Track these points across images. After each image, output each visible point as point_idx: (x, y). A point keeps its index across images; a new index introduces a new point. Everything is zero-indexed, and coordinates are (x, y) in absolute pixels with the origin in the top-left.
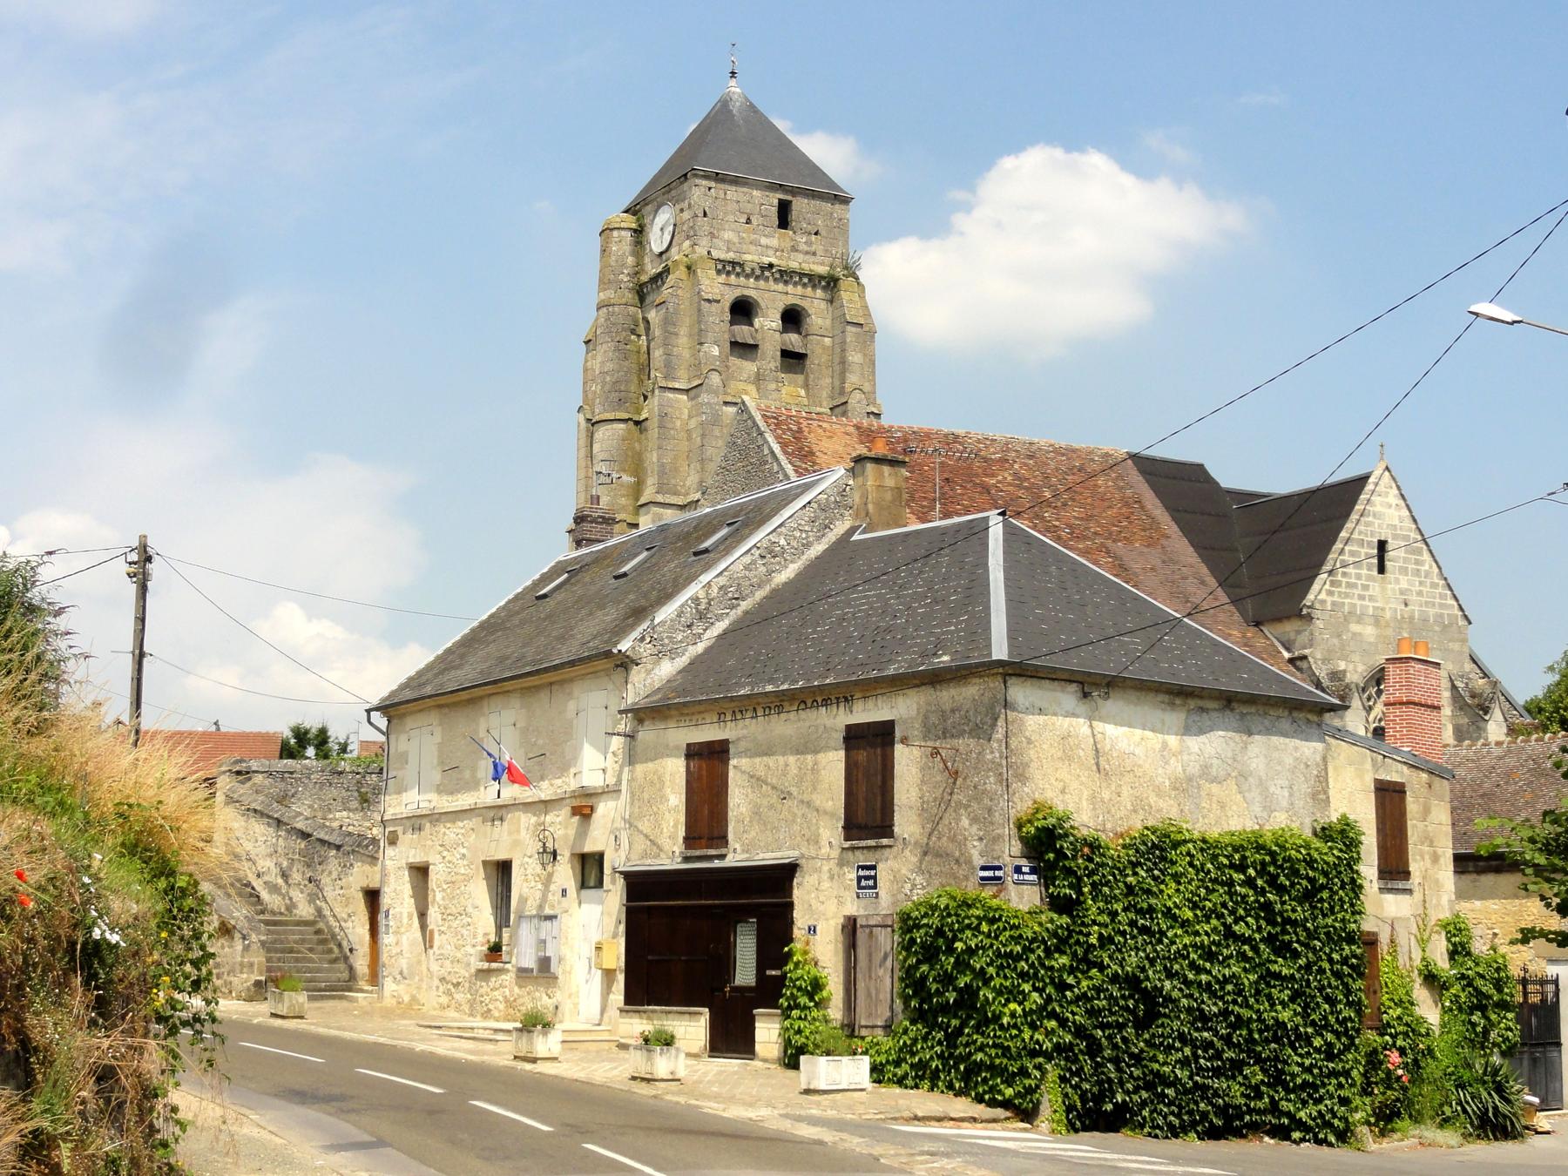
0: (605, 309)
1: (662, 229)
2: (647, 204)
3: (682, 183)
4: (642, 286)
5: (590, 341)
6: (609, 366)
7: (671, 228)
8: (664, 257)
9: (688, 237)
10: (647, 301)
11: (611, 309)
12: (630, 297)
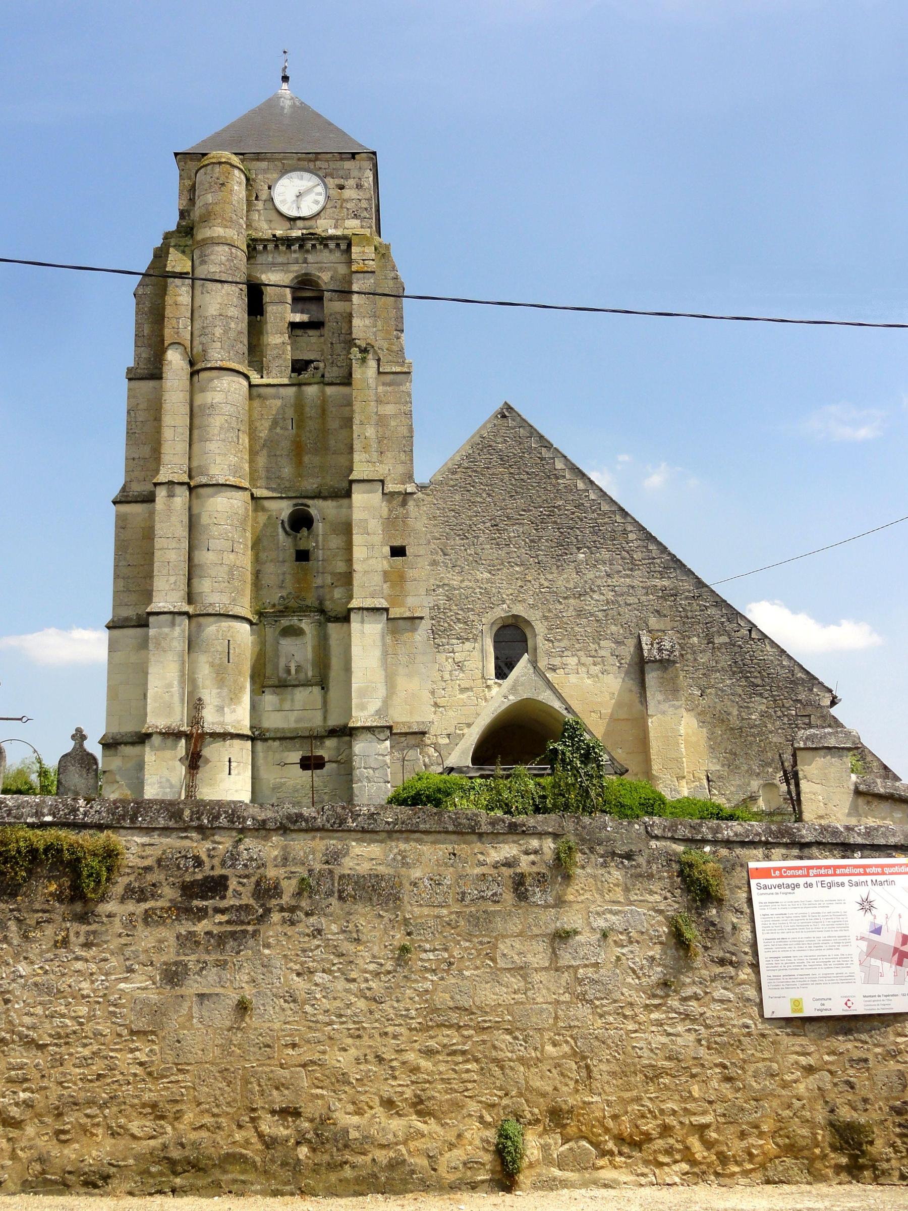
0: (226, 248)
2: (258, 160)
3: (342, 159)
4: (254, 240)
8: (300, 223)
9: (356, 216)
10: (261, 259)
11: (234, 250)
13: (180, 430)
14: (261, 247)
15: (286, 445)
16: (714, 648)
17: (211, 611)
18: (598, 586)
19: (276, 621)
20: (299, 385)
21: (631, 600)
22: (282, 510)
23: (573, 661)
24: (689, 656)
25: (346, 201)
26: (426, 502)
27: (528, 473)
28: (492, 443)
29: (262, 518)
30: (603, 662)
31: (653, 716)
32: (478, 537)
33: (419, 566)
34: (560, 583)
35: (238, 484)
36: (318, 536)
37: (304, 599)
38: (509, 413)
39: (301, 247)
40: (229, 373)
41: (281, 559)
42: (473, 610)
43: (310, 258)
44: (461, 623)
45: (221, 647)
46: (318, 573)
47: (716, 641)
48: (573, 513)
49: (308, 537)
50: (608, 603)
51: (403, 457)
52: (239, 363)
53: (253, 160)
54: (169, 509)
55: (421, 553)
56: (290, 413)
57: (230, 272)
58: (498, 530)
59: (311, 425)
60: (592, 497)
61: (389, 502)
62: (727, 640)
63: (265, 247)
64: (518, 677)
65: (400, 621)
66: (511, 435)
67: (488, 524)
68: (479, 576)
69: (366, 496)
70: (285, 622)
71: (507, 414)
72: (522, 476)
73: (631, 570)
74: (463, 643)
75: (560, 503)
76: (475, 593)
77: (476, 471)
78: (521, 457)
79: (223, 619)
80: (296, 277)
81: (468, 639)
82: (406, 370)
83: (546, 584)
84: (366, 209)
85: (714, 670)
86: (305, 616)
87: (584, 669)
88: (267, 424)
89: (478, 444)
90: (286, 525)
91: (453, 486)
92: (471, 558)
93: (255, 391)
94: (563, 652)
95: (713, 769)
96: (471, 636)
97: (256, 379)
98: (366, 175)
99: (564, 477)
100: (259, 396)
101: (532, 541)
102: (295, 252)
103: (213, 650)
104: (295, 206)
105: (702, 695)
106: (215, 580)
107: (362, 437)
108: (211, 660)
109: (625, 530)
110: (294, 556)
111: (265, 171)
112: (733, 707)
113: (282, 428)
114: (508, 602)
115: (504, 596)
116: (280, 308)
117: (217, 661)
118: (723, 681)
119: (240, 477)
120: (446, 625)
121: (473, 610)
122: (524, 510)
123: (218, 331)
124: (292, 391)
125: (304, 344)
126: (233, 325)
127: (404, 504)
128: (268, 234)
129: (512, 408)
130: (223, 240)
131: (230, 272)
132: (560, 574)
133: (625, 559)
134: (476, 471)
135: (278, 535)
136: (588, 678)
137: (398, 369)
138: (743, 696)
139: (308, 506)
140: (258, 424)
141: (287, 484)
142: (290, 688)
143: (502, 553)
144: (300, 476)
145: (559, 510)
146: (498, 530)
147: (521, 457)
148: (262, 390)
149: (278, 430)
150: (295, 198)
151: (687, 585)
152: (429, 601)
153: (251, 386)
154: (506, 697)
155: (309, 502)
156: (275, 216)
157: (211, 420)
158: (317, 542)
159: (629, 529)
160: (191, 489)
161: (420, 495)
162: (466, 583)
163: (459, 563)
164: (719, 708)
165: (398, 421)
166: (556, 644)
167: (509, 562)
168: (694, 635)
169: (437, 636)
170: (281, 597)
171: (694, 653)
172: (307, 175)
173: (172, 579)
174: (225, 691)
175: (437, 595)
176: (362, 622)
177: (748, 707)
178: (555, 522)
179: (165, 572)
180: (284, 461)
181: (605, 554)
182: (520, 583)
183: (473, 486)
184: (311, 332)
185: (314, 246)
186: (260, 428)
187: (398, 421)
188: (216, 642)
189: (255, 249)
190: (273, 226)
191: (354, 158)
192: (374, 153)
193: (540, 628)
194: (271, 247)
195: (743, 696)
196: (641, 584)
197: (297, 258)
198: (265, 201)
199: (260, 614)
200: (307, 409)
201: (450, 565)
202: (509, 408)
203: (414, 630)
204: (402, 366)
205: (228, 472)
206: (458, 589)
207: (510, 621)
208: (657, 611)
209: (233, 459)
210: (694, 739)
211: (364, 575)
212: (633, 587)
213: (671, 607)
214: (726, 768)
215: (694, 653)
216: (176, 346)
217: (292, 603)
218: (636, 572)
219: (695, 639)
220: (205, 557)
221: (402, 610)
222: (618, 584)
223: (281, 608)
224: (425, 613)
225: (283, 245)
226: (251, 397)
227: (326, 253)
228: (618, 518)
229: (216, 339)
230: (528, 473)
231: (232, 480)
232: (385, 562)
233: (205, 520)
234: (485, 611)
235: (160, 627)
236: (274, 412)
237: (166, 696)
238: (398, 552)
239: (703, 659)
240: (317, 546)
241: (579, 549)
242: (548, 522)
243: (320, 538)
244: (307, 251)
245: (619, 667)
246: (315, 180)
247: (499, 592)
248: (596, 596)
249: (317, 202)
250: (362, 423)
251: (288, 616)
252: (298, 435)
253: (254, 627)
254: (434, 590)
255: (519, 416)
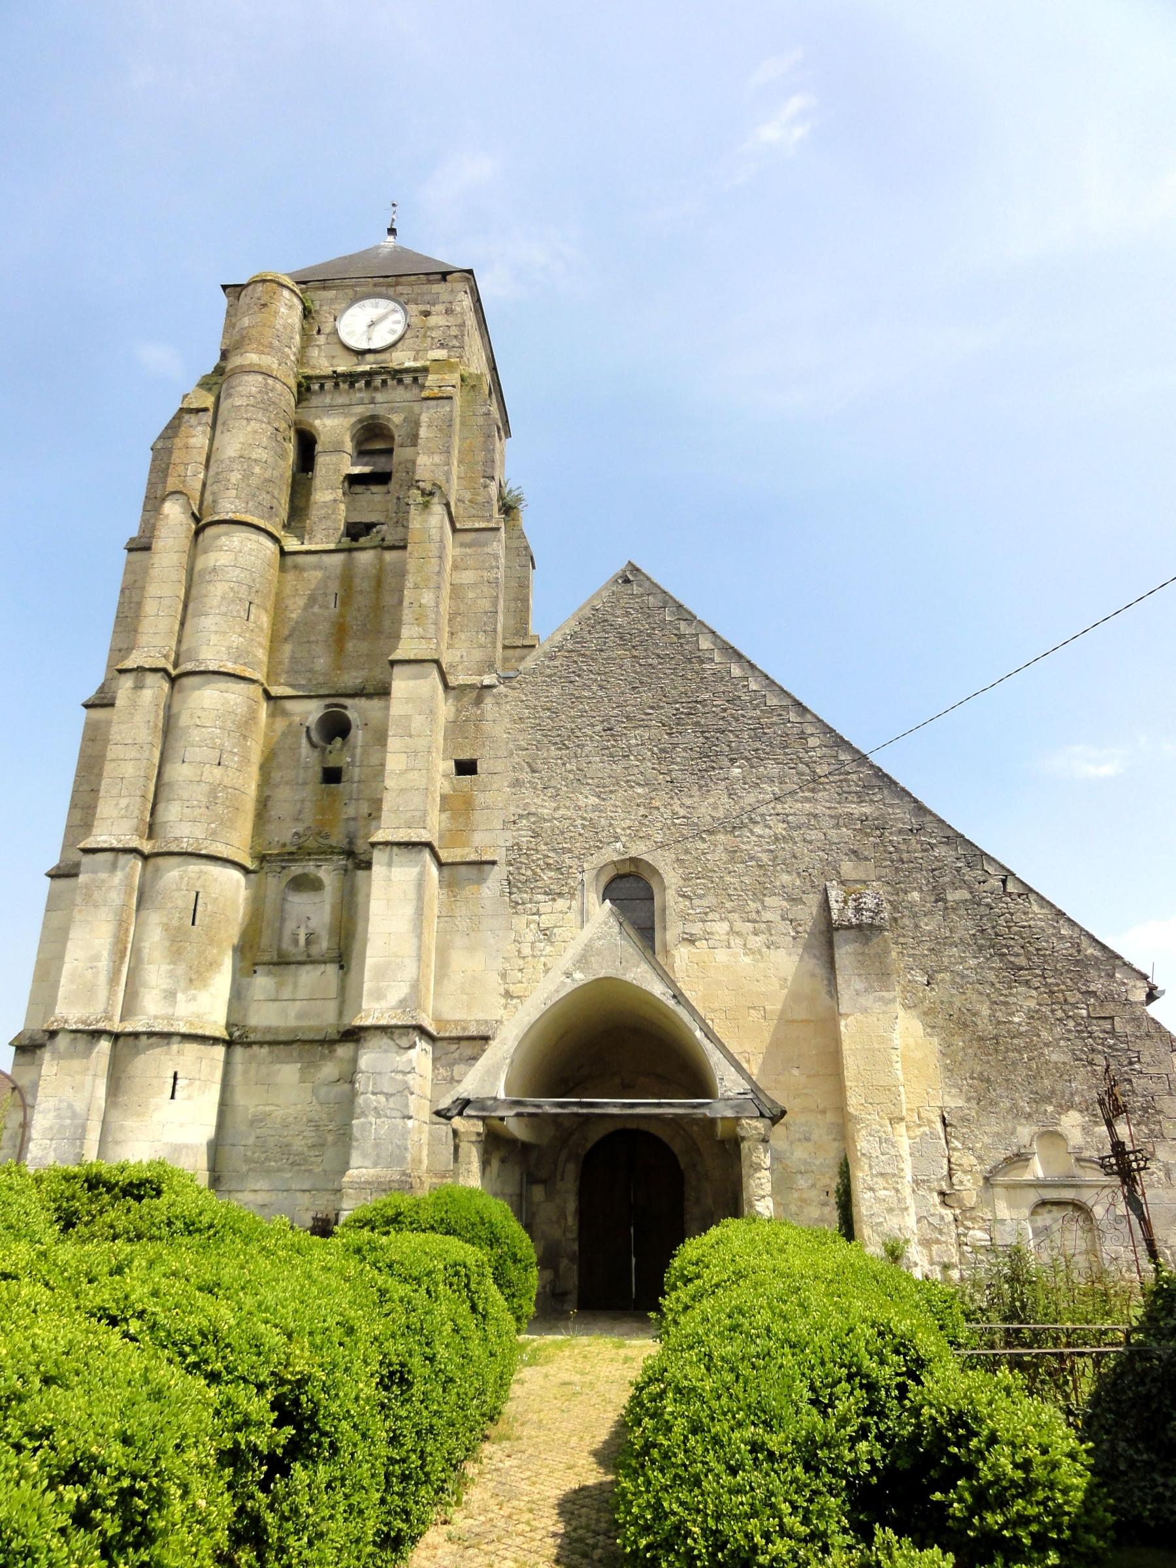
0: (260, 378)
1: (372, 324)
2: (324, 288)
3: (429, 282)
4: (308, 378)
5: (205, 410)
6: (260, 454)
7: (400, 329)
9: (442, 346)
10: (315, 401)
11: (270, 381)
12: (292, 383)
13: (167, 602)
14: (316, 387)
15: (324, 627)
16: (946, 908)
17: (174, 848)
18: (762, 815)
19: (284, 868)
20: (350, 550)
21: (813, 835)
22: (309, 713)
23: (721, 928)
24: (906, 921)
25: (431, 329)
26: (509, 699)
27: (658, 656)
28: (609, 617)
29: (280, 724)
30: (769, 931)
31: (847, 1015)
32: (583, 745)
33: (495, 787)
34: (703, 810)
35: (238, 672)
36: (355, 747)
37: (327, 837)
38: (635, 575)
39: (368, 384)
40: (244, 528)
41: (300, 781)
42: (570, 851)
43: (379, 397)
44: (551, 870)
45: (184, 901)
46: (351, 799)
47: (949, 898)
48: (725, 710)
49: (341, 749)
50: (777, 839)
51: (482, 638)
52: (262, 517)
53: (318, 289)
54: (134, 704)
55: (499, 769)
56: (334, 586)
57: (262, 405)
58: (612, 735)
59: (361, 601)
60: (753, 686)
61: (458, 699)
62: (968, 896)
63: (322, 386)
64: (591, 940)
65: (463, 869)
66: (636, 606)
67: (599, 728)
68: (582, 802)
69: (411, 683)
70: (296, 869)
71: (631, 577)
72: (650, 661)
73: (813, 790)
74: (554, 900)
75: (706, 696)
76: (575, 826)
77: (584, 655)
78: (649, 635)
79: (194, 860)
80: (360, 421)
81: (560, 895)
82: (494, 526)
83: (682, 812)
84: (456, 337)
85: (947, 942)
86: (326, 860)
87: (739, 941)
88: (301, 602)
89: (589, 619)
90: (315, 737)
91: (549, 676)
92: (572, 776)
93: (290, 560)
94: (706, 914)
95: (953, 1105)
96: (566, 889)
97: (292, 544)
98: (459, 298)
99: (712, 660)
100: (296, 567)
101: (663, 751)
102: (360, 390)
103: (170, 905)
104: (365, 337)
105: (929, 984)
106: (187, 804)
107: (416, 605)
108: (165, 920)
109: (803, 733)
110: (320, 775)
111: (332, 301)
112: (982, 1002)
113: (321, 607)
114: (623, 839)
115: (618, 830)
116: (333, 458)
117: (175, 923)
118: (963, 960)
119: (245, 664)
120: (529, 873)
121: (570, 851)
122: (652, 708)
123: (235, 477)
124: (339, 558)
125: (364, 503)
126: (257, 470)
127: (478, 701)
128: (328, 371)
129: (638, 570)
130: (256, 369)
131: (262, 405)
132: (703, 797)
133: (803, 774)
134: (584, 655)
135: (300, 747)
136: (745, 954)
137: (483, 525)
138: (998, 985)
139: (345, 708)
140: (289, 602)
141: (321, 679)
142: (293, 967)
143: (618, 768)
144: (339, 669)
145: (704, 706)
146: (612, 735)
147: (649, 635)
148: (300, 559)
149: (316, 609)
150: (365, 328)
151: (902, 816)
152: (505, 838)
153: (283, 553)
154: (568, 975)
155: (348, 702)
156: (339, 351)
157: (211, 588)
158: (353, 756)
159: (809, 731)
160: (173, 680)
161: (502, 689)
162: (562, 812)
163: (553, 783)
164: (958, 1004)
165: (479, 591)
166: (696, 902)
167: (628, 781)
168: (914, 889)
169: (515, 890)
170: (296, 833)
171: (915, 916)
172: (383, 302)
173: (123, 802)
174: (181, 969)
175: (518, 830)
176: (390, 864)
177: (1006, 1003)
178: (697, 724)
179: (114, 792)
180: (319, 649)
181: (773, 769)
182: (642, 811)
183: (579, 676)
184: (375, 488)
185: (384, 382)
186: (292, 608)
187: (479, 591)
188: (176, 894)
189: (308, 389)
190: (335, 362)
191: (444, 280)
192: (470, 272)
193: (671, 877)
194: (329, 385)
195: (998, 985)
196: (828, 812)
197: (362, 398)
198: (328, 334)
199: (262, 858)
200: (357, 581)
201: (539, 786)
202: (635, 570)
203: (481, 881)
204: (488, 521)
205: (225, 657)
206: (549, 821)
207: (626, 869)
208: (854, 852)
209: (236, 640)
210: (918, 1054)
211: (398, 795)
212: (815, 816)
213: (875, 845)
214: (974, 1104)
215: (915, 916)
216: (177, 496)
217: (311, 843)
218: (820, 794)
219: (916, 895)
220: (179, 772)
221: (467, 850)
222: (792, 811)
223: (293, 849)
224: (499, 855)
225: (344, 382)
226: (283, 568)
227: (400, 390)
228: (793, 716)
229: (230, 486)
230: (658, 656)
231: (230, 667)
232: (446, 783)
233: (184, 720)
234: (588, 852)
235: (95, 872)
236: (313, 587)
237: (89, 974)
238: (466, 768)
239: (928, 925)
240: (352, 763)
241: (733, 761)
242: (688, 724)
243: (358, 751)
244: (376, 389)
245: (794, 938)
246: (392, 305)
247: (611, 825)
248: (758, 830)
249: (393, 332)
250: (416, 587)
251: (301, 860)
252: (342, 615)
253: (252, 876)
254: (514, 823)
255: (648, 579)
